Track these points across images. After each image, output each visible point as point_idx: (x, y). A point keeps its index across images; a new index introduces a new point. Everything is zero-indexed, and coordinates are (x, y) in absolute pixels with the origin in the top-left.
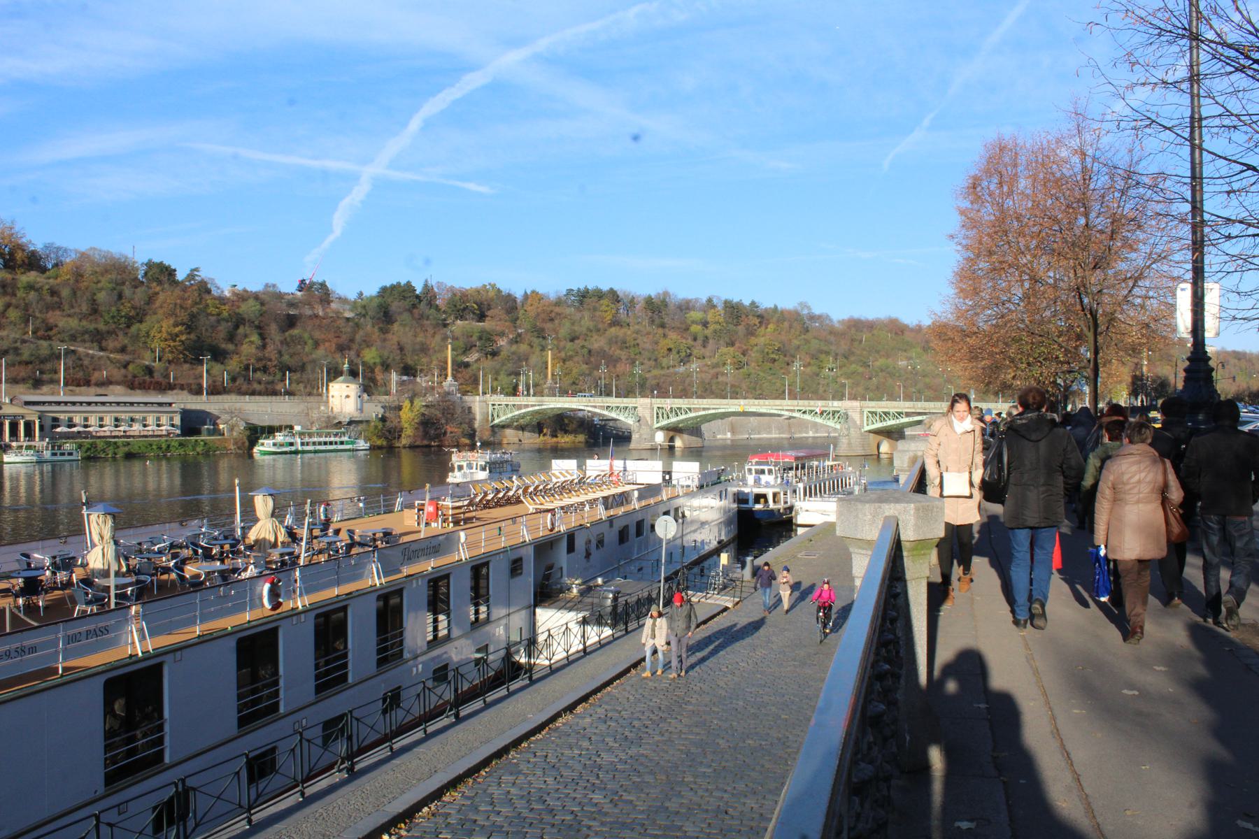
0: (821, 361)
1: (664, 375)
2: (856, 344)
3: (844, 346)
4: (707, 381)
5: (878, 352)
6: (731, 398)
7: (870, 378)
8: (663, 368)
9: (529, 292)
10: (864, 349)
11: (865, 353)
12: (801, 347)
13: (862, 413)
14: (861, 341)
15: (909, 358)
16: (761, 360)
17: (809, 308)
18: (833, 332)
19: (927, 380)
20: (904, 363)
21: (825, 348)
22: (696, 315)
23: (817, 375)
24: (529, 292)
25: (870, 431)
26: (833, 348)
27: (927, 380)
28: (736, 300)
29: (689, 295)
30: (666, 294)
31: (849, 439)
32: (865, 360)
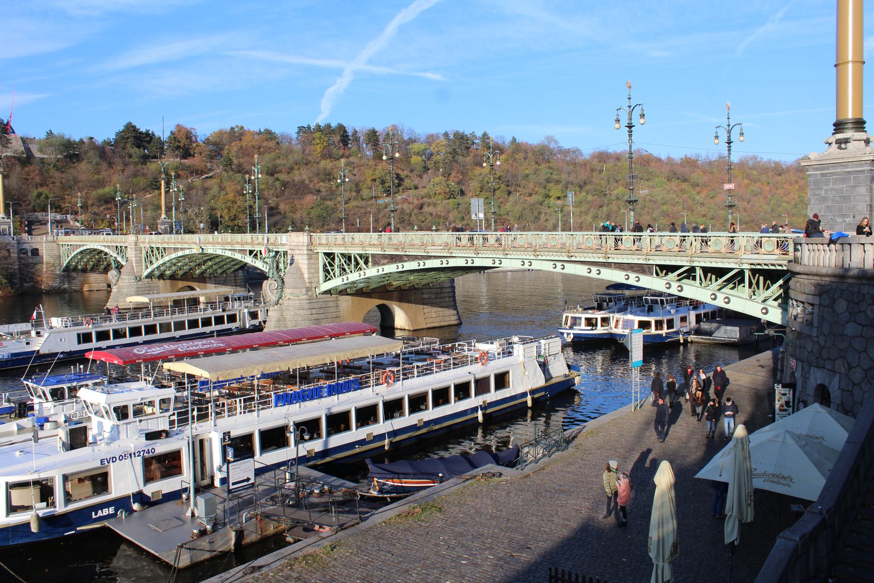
1: (357, 207)
2: (595, 174)
3: (583, 175)
4: (408, 211)
5: (617, 182)
7: (601, 207)
9: (262, 130)
10: (603, 179)
11: (603, 182)
12: (530, 176)
13: (312, 255)
15: (649, 187)
16: (479, 189)
17: (556, 142)
18: (584, 164)
19: (665, 208)
20: (646, 192)
21: (555, 177)
22: (415, 147)
23: (541, 204)
24: (262, 130)
25: (328, 292)
26: (564, 176)
27: (665, 208)
28: (461, 131)
30: (395, 127)
31: (281, 310)
32: (603, 189)
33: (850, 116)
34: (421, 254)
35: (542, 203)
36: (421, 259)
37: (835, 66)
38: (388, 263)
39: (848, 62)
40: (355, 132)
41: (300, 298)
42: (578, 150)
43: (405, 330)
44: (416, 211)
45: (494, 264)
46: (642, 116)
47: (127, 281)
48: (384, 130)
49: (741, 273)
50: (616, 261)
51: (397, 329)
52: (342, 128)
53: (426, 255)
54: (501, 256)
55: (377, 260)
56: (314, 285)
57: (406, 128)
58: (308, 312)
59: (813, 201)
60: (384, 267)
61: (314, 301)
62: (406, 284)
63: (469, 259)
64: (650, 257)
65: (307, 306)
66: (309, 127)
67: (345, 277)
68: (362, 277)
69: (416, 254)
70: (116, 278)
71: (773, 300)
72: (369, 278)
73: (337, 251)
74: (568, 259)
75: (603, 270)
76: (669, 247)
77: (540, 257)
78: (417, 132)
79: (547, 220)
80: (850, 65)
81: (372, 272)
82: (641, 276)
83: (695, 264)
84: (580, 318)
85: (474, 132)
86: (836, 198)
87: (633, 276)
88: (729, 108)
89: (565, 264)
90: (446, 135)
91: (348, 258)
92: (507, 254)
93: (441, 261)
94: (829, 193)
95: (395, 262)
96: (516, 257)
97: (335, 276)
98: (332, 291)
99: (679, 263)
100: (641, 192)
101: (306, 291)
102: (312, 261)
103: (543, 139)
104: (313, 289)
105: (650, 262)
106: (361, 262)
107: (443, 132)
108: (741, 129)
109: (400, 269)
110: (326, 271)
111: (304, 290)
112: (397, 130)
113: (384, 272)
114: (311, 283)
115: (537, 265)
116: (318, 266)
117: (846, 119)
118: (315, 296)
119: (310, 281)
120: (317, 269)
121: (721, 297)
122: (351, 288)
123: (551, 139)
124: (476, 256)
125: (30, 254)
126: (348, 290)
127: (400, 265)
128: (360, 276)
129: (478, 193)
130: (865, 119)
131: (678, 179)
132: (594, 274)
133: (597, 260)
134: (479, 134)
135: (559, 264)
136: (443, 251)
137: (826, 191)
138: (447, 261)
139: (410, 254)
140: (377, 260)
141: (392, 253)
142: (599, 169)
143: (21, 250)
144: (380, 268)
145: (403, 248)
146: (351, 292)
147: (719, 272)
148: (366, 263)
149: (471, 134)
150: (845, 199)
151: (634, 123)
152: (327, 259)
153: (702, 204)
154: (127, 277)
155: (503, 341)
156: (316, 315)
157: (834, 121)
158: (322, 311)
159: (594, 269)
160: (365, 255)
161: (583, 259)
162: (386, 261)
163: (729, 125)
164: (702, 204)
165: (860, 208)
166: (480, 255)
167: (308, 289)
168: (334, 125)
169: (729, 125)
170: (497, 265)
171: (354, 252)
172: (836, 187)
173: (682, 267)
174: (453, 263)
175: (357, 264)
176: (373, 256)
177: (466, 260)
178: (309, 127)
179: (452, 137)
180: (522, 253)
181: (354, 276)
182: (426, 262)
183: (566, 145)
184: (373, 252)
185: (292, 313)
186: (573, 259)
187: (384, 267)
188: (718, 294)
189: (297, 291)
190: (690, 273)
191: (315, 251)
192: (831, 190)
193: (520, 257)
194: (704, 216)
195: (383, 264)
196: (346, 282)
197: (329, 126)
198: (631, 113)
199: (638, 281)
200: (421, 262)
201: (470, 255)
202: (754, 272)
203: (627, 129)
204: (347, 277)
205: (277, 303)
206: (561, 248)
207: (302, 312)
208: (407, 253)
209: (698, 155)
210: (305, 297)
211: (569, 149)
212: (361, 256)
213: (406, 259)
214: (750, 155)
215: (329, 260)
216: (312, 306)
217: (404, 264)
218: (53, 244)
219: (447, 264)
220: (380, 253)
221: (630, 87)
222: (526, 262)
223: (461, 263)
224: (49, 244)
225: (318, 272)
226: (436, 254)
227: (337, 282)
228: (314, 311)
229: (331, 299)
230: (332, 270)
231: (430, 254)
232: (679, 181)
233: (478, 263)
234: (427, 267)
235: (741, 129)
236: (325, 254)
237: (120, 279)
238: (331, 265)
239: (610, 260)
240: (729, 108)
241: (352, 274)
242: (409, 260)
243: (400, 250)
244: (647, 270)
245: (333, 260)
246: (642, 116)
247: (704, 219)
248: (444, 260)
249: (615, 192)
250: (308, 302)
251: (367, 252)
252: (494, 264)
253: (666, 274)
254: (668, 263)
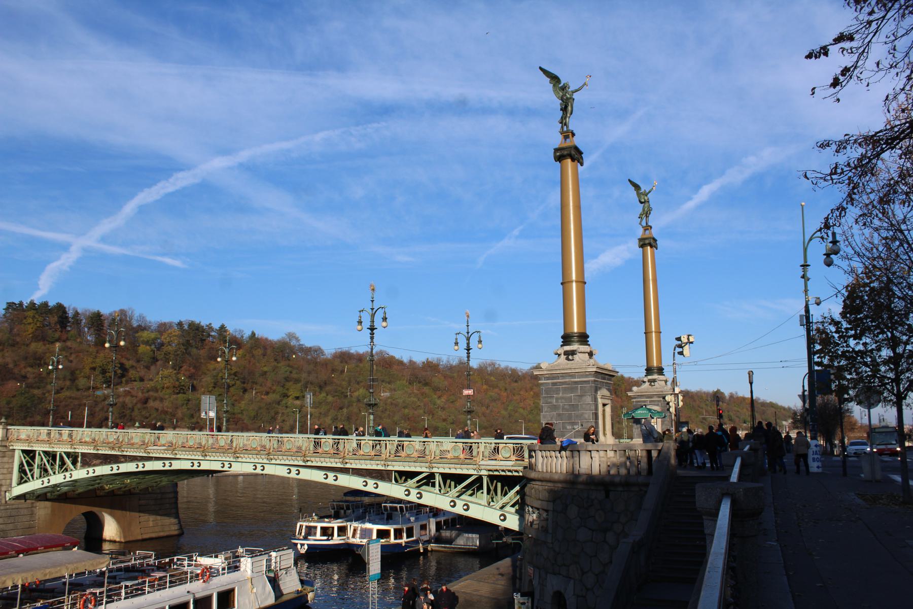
0: (288, 389)
1: (70, 398)
4: (130, 406)
5: (358, 383)
6: (116, 426)
7: (341, 408)
8: (78, 390)
10: (344, 380)
11: (344, 383)
12: (268, 374)
14: (343, 371)
15: (391, 390)
16: (212, 385)
17: (297, 339)
18: (326, 364)
19: (406, 411)
20: (388, 394)
21: (294, 375)
22: (145, 335)
23: (279, 403)
28: (197, 321)
29: (166, 320)
30: (123, 312)
32: (343, 390)
33: (576, 330)
34: (141, 454)
35: (279, 402)
36: (140, 461)
37: (562, 284)
38: (101, 464)
39: (572, 282)
40: (77, 314)
42: (320, 349)
43: (115, 542)
44: (139, 406)
45: (223, 467)
46: (385, 319)
48: (111, 314)
49: (479, 479)
50: (354, 466)
51: (106, 541)
52: (60, 308)
53: (146, 455)
54: (232, 459)
55: (88, 460)
57: (136, 314)
59: (545, 409)
60: (96, 468)
62: (120, 488)
63: (195, 462)
64: (389, 463)
66: (21, 304)
67: (46, 480)
68: (68, 479)
69: (135, 454)
71: (511, 506)
72: (75, 481)
73: (38, 448)
74: (304, 464)
75: (340, 476)
76: (408, 453)
77: (274, 461)
78: (148, 319)
79: (284, 421)
80: (574, 284)
81: (80, 474)
82: (380, 483)
83: (435, 470)
84: (316, 527)
85: (210, 324)
86: (566, 407)
87: (371, 482)
88: (468, 316)
89: (300, 469)
90: (180, 324)
91: (51, 456)
92: (238, 457)
93: (164, 463)
94: (560, 401)
95: (110, 463)
96: (248, 460)
97: (33, 478)
98: (27, 496)
99: (418, 469)
100: (382, 395)
103: (284, 336)
105: (390, 468)
106: (68, 462)
107: (176, 321)
108: (480, 337)
109: (115, 471)
110: (22, 471)
112: (126, 316)
113: (96, 474)
115: (270, 470)
116: (13, 465)
117: (572, 333)
120: (10, 470)
121: (460, 503)
122: (52, 492)
123: (291, 336)
124: (203, 458)
126: (49, 495)
127: (115, 466)
128: (65, 479)
129: (210, 389)
130: (588, 333)
131: (420, 382)
132: (330, 480)
133: (334, 465)
134: (216, 326)
135: (294, 469)
136: (166, 451)
137: (557, 399)
138: (170, 463)
139: (128, 454)
140: (88, 460)
141: (106, 452)
142: (340, 369)
144: (91, 470)
145: (119, 447)
146: (52, 497)
147: (458, 479)
148: (74, 463)
149: (207, 326)
150: (574, 407)
151: (376, 325)
152: (25, 458)
153: (443, 409)
155: (229, 554)
157: (562, 333)
158: (12, 520)
159: (331, 475)
160: (73, 454)
161: (319, 464)
162: (98, 461)
163: (468, 333)
164: (443, 409)
165: (586, 416)
166: (208, 458)
168: (52, 304)
169: (468, 333)
170: (226, 468)
171: (61, 450)
172: (564, 395)
173: (421, 473)
174: (177, 465)
175: (63, 463)
176: (83, 455)
177: (192, 463)
178: (21, 304)
179: (186, 327)
180: (254, 456)
181: (57, 479)
182: (146, 463)
183: (308, 343)
184: (83, 451)
186: (309, 464)
187: (95, 468)
188: (456, 500)
190: (429, 480)
191: (11, 448)
192: (562, 398)
193: (252, 460)
194: (444, 420)
195: (95, 465)
196: (46, 484)
197: (45, 305)
198: (373, 316)
199: (376, 488)
200: (140, 464)
201: (197, 457)
202: (492, 478)
203: (370, 331)
204: (49, 479)
206: (296, 452)
208: (125, 453)
209: (439, 360)
211: (310, 348)
212: (68, 454)
213: (123, 460)
214: (488, 362)
215: (27, 458)
217: (119, 465)
219: (170, 466)
220: (92, 451)
221: (373, 290)
222: (259, 466)
223: (186, 465)
225: (11, 473)
226: (158, 455)
227: (34, 485)
229: (25, 506)
230: (31, 470)
231: (151, 455)
232: (421, 384)
233: (205, 466)
234: (120, 471)
235: (480, 337)
236: (24, 451)
238: (29, 464)
239: (348, 466)
240: (468, 316)
241: (55, 476)
242: (125, 461)
243: (117, 449)
244: (386, 476)
245: (33, 458)
246: (385, 319)
247: (444, 423)
248: (167, 462)
249: (356, 394)
251: (77, 451)
252: (223, 467)
253: (406, 481)
254: (407, 469)
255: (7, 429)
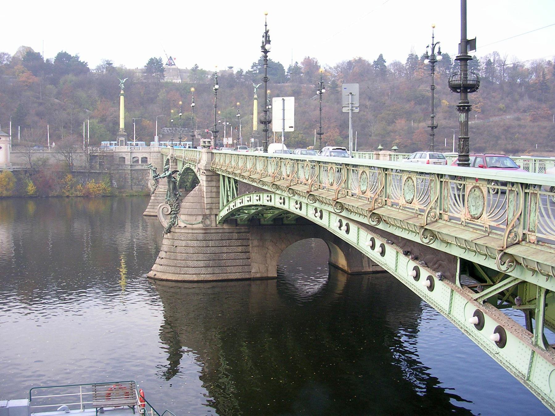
41: (195, 226)
47: (163, 190)
56: (214, 212)
58: (204, 243)
61: (212, 231)
65: (201, 237)
70: (154, 187)
101: (203, 219)
102: (214, 184)
104: (213, 217)
111: (200, 218)
114: (211, 209)
118: (214, 224)
119: (208, 207)
125: (140, 162)
143: (133, 158)
146: (266, 223)
154: (163, 186)
156: (213, 248)
167: (205, 217)
185: (184, 243)
189: (192, 219)
205: (169, 231)
207: (195, 243)
210: (201, 226)
216: (209, 237)
218: (158, 154)
224: (154, 154)
228: (211, 243)
237: (157, 188)
250: (203, 232)
255: (212, 153)
